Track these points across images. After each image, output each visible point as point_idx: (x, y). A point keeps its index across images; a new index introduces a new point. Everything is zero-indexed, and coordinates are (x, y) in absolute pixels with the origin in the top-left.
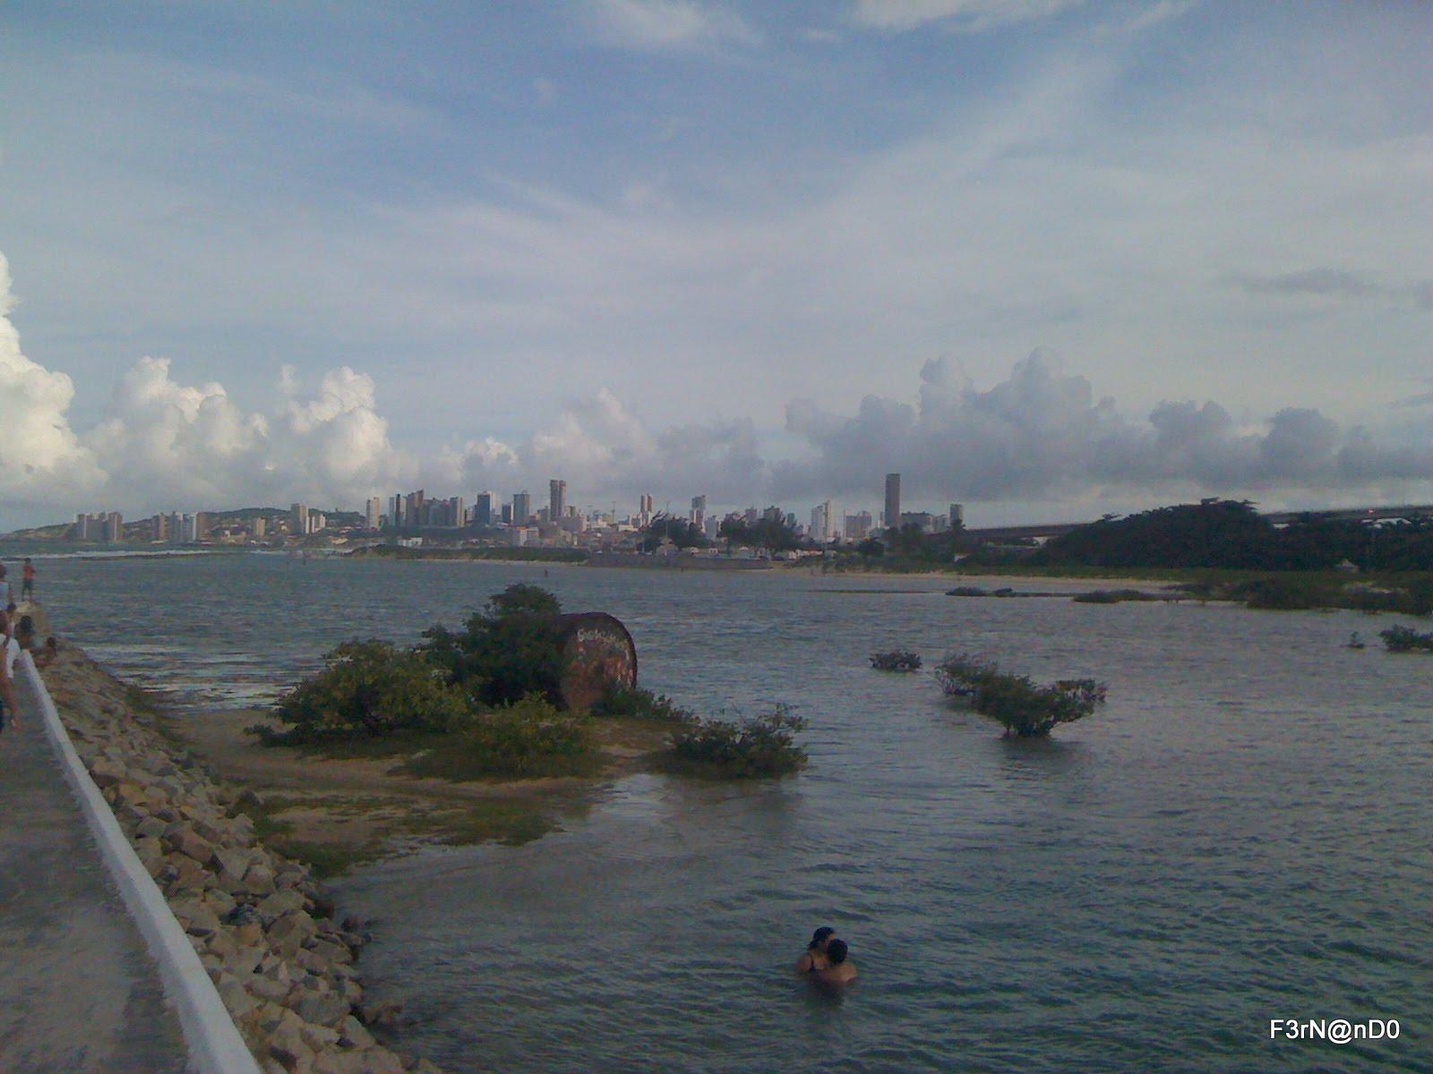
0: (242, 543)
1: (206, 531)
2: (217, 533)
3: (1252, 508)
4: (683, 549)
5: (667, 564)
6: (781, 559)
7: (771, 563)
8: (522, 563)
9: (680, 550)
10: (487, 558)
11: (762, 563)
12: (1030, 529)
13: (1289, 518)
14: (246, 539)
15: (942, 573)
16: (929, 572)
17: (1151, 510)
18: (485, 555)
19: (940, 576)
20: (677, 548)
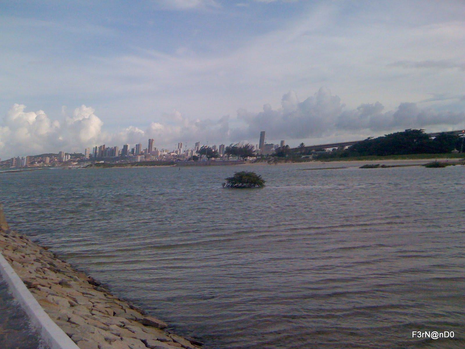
0: (41, 166)
1: (29, 163)
2: (32, 163)
3: (423, 132)
4: (210, 159)
5: (206, 164)
6: (246, 160)
7: (245, 162)
8: (152, 167)
9: (209, 159)
10: (137, 166)
11: (241, 162)
12: (344, 143)
13: (436, 135)
14: (42, 164)
15: (315, 161)
16: (309, 162)
17: (387, 134)
18: (136, 165)
19: (314, 162)
20: (207, 159)
